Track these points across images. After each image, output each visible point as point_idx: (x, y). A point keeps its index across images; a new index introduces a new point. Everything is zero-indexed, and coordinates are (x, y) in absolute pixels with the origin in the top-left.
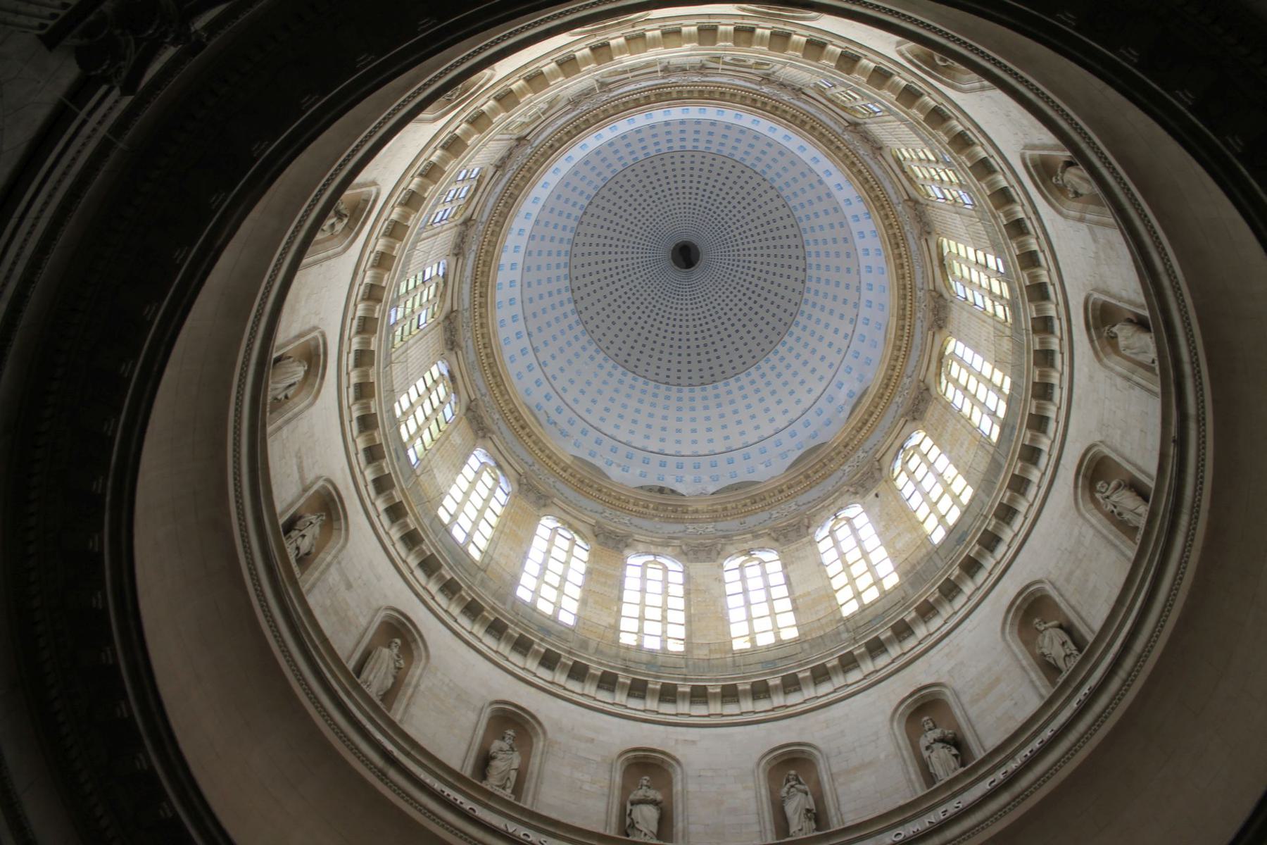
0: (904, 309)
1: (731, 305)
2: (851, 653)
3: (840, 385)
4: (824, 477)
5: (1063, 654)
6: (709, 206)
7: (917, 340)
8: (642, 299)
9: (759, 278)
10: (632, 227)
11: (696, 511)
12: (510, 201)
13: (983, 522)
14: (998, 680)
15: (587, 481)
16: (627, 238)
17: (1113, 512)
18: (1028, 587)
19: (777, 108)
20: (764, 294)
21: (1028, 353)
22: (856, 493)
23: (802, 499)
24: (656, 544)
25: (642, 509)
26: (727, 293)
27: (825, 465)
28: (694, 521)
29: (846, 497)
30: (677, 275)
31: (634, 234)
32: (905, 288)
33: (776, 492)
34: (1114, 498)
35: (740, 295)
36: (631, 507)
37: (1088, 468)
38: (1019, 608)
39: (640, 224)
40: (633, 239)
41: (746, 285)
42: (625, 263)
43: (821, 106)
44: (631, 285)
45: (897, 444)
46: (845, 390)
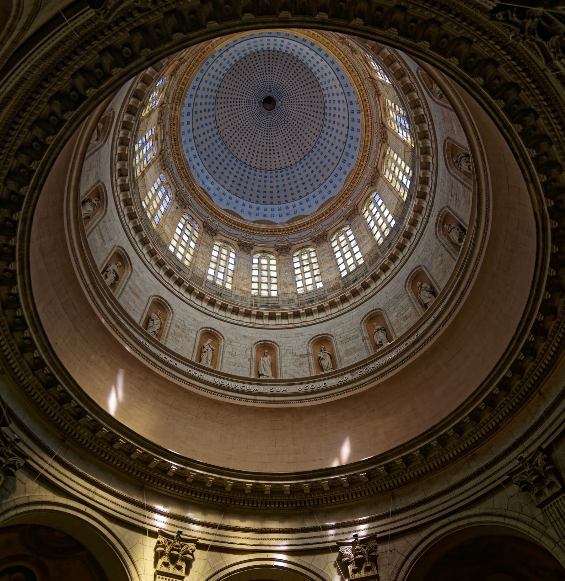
0: (245, 228)
1: (242, 120)
2: (136, 217)
3: (212, 183)
4: (181, 177)
5: (155, 330)
6: (288, 124)
7: (233, 231)
8: (257, 75)
9: (250, 137)
10: (291, 83)
11: (175, 109)
12: (350, 70)
13: (187, 280)
14: (138, 297)
15: (204, 56)
16: (287, 79)
17: (204, 348)
18: (170, 305)
19: (340, 202)
20: (244, 138)
21: (250, 308)
22: (176, 195)
23: (173, 164)
24: (167, 89)
25: (182, 81)
26: (247, 119)
27: (186, 178)
28: (172, 108)
29: (174, 189)
30: (263, 96)
31: (287, 83)
32: (254, 230)
33: (178, 152)
34: (210, 349)
35: (245, 125)
36: (185, 76)
37: (213, 333)
38: (161, 301)
39: (291, 88)
40: (285, 81)
41: (249, 130)
42: (276, 73)
43: (337, 223)
44: (264, 73)
45: (194, 217)
46: (211, 186)
